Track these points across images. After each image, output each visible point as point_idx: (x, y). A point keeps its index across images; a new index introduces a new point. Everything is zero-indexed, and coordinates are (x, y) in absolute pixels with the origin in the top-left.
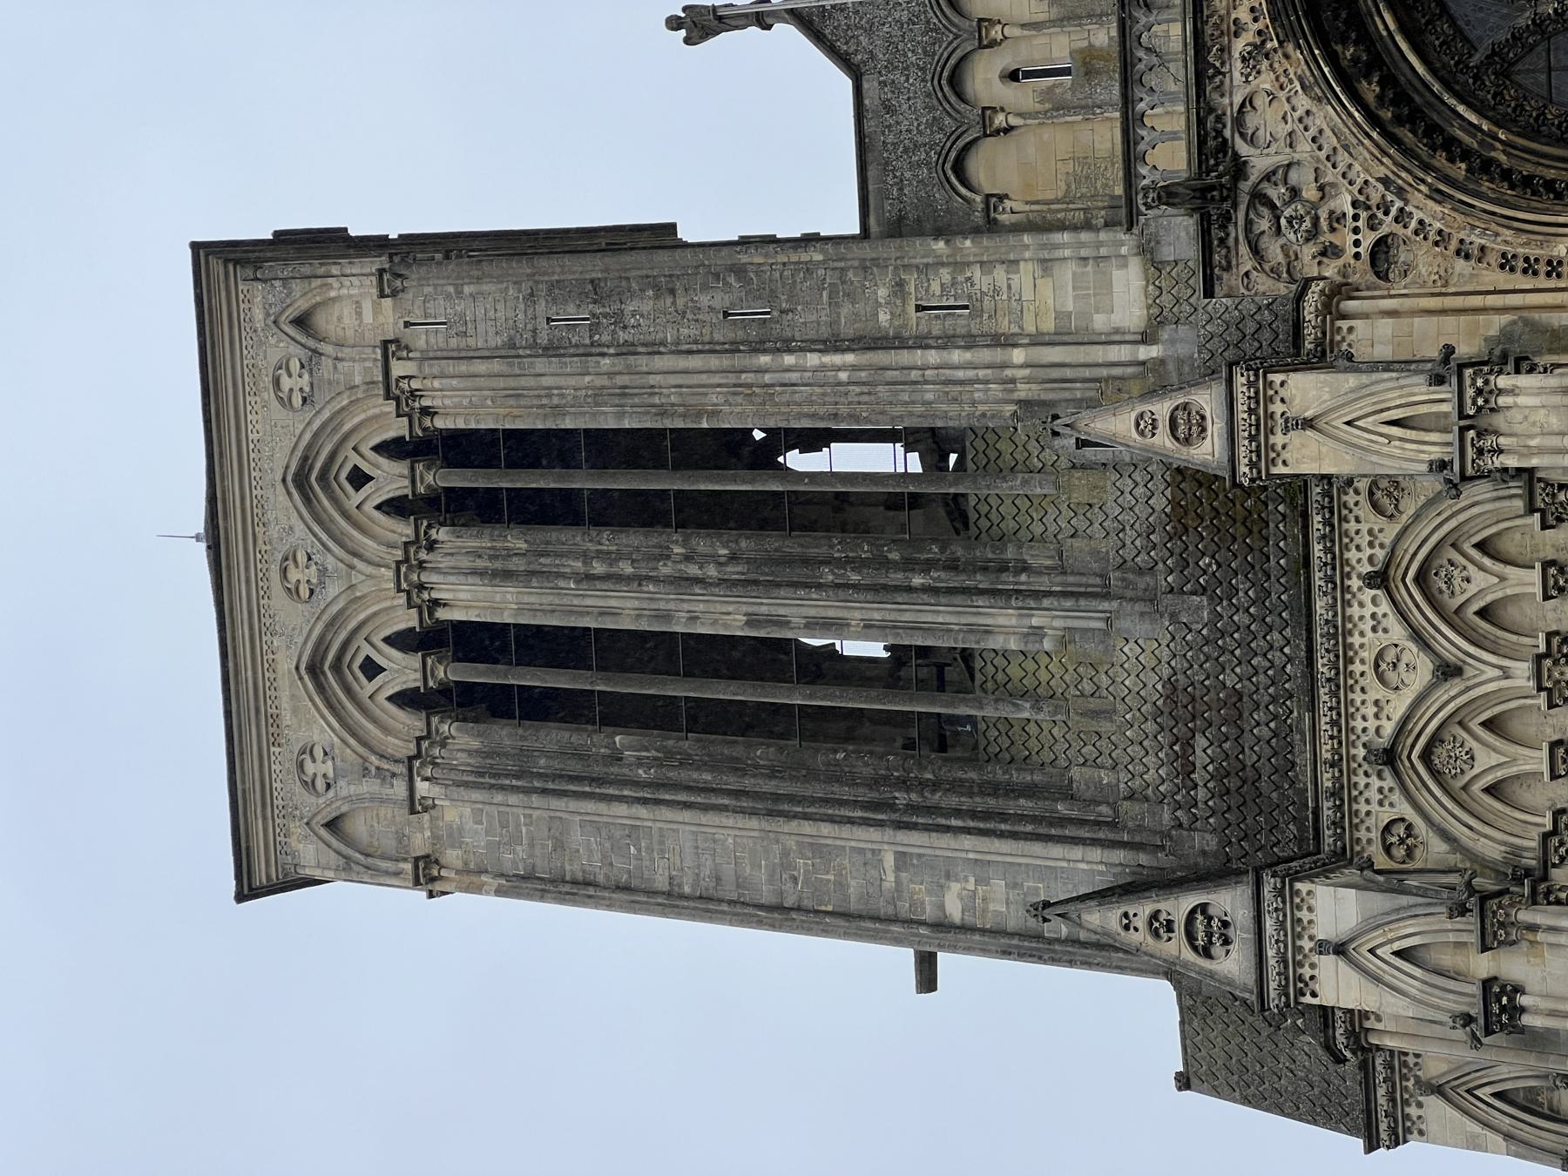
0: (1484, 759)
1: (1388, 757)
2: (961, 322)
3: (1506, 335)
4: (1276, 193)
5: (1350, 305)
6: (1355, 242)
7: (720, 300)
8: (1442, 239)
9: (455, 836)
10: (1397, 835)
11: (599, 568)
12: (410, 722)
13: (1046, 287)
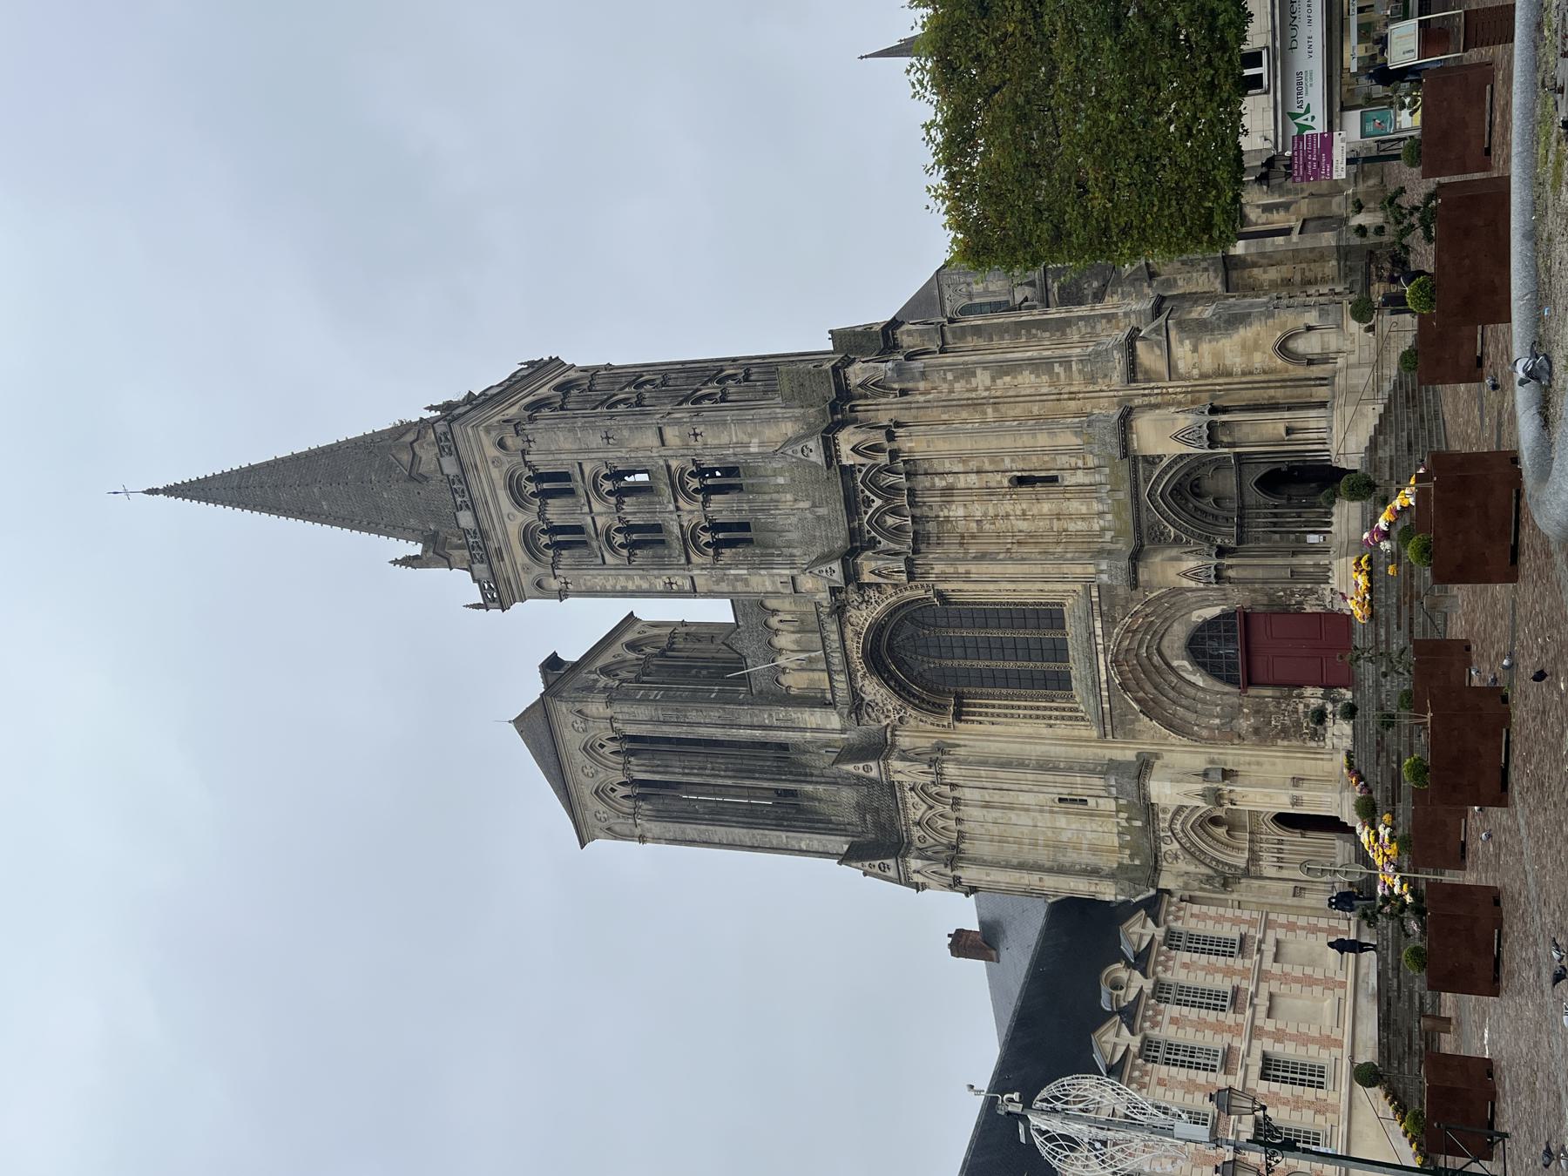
0: (939, 822)
1: (919, 824)
2: (789, 724)
3: (937, 743)
4: (873, 704)
5: (897, 733)
6: (895, 717)
7: (717, 714)
8: (916, 718)
9: (650, 830)
10: (922, 839)
11: (686, 771)
12: (630, 803)
13: (812, 718)
